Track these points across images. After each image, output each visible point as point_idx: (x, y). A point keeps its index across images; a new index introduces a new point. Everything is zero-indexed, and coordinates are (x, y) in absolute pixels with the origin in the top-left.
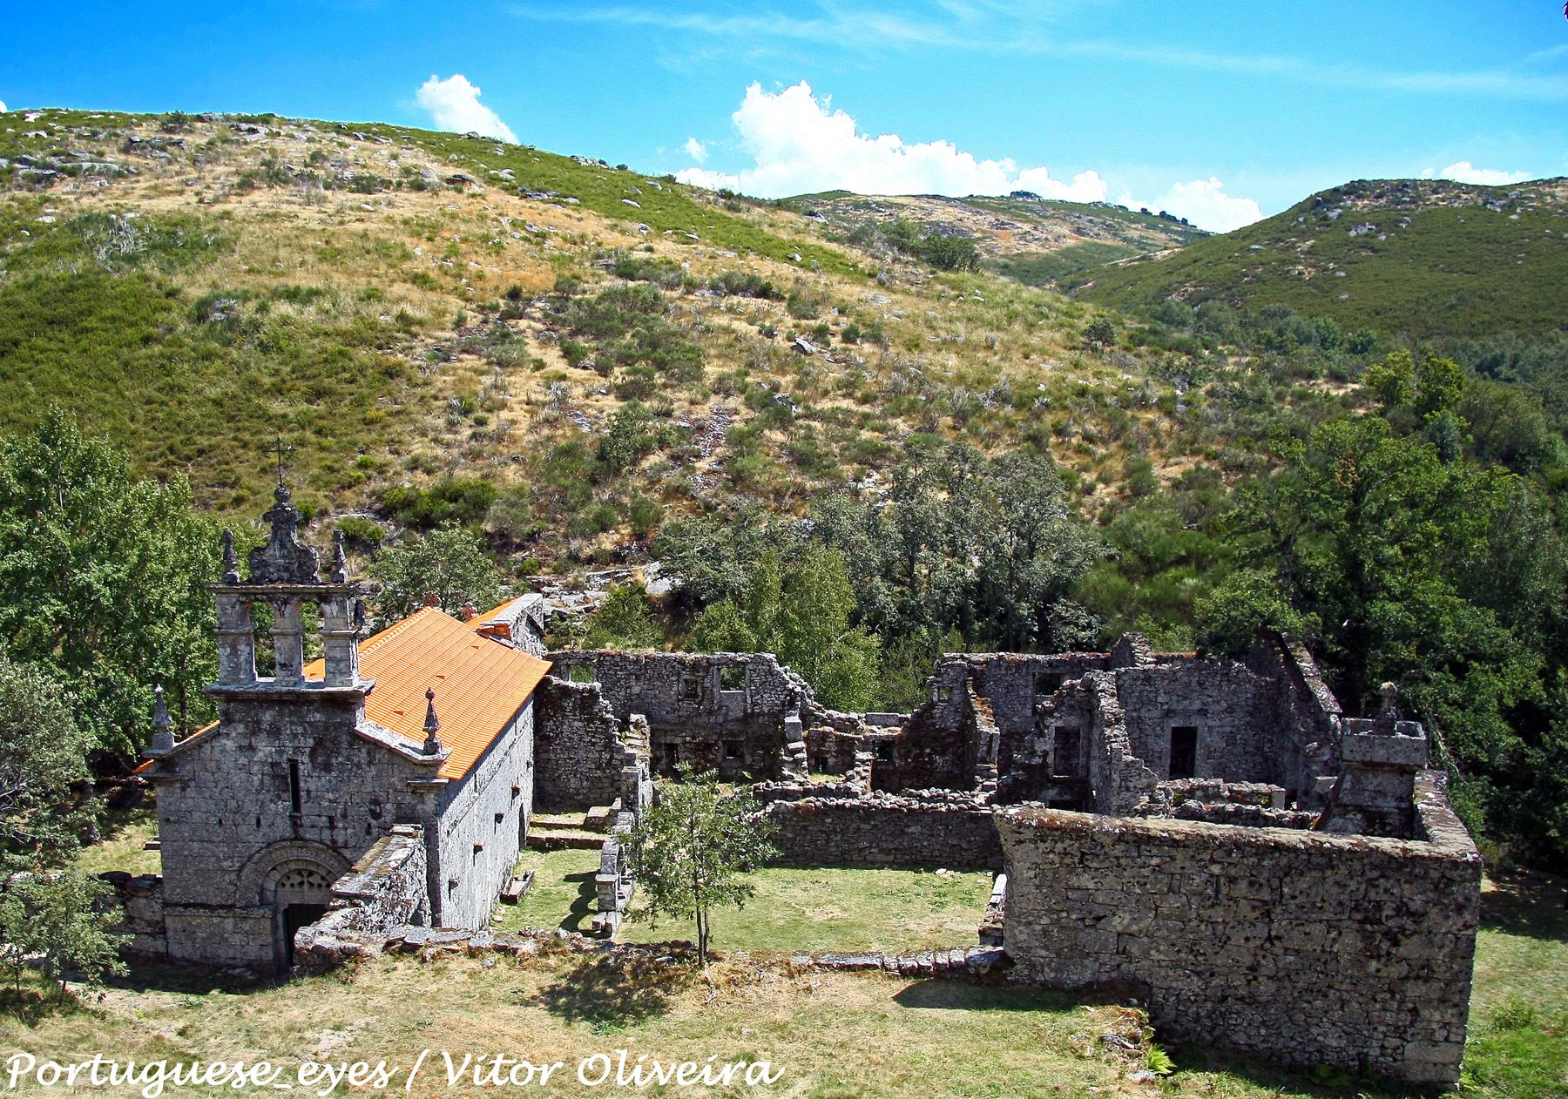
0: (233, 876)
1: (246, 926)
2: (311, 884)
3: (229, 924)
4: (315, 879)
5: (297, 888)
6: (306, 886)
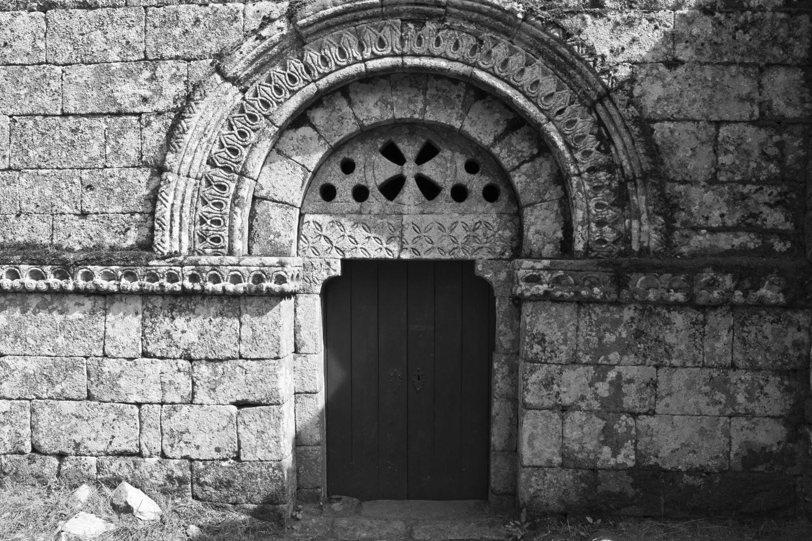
0: (155, 134)
1: (188, 329)
2: (429, 189)
3: (124, 327)
4: (445, 169)
5: (376, 202)
6: (411, 190)
